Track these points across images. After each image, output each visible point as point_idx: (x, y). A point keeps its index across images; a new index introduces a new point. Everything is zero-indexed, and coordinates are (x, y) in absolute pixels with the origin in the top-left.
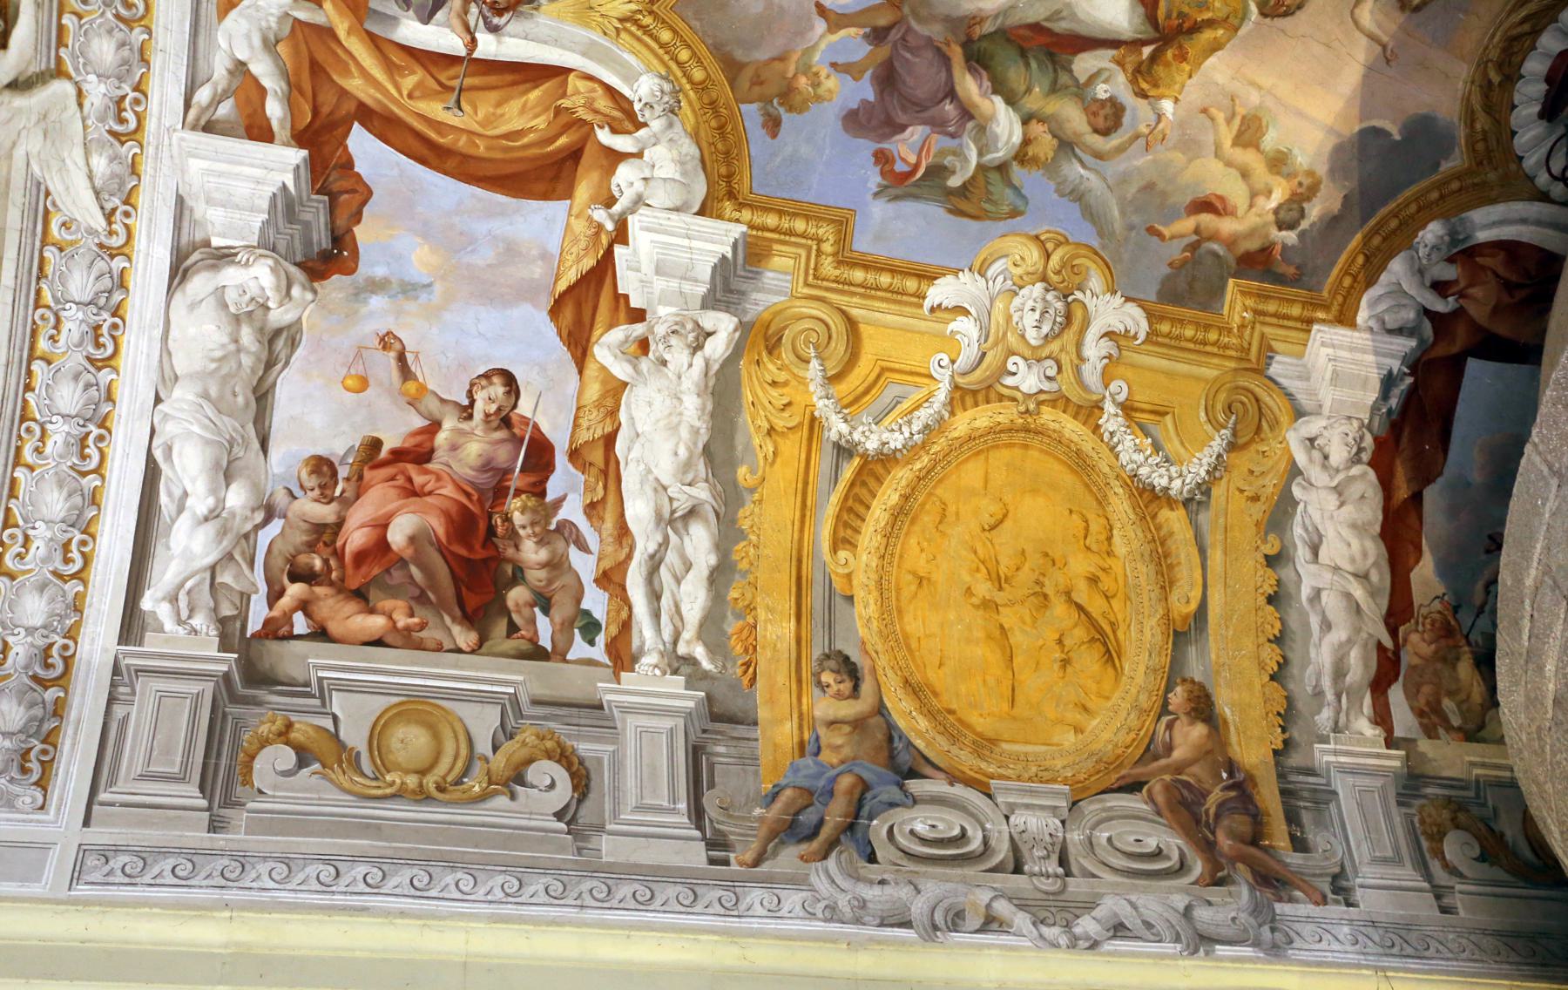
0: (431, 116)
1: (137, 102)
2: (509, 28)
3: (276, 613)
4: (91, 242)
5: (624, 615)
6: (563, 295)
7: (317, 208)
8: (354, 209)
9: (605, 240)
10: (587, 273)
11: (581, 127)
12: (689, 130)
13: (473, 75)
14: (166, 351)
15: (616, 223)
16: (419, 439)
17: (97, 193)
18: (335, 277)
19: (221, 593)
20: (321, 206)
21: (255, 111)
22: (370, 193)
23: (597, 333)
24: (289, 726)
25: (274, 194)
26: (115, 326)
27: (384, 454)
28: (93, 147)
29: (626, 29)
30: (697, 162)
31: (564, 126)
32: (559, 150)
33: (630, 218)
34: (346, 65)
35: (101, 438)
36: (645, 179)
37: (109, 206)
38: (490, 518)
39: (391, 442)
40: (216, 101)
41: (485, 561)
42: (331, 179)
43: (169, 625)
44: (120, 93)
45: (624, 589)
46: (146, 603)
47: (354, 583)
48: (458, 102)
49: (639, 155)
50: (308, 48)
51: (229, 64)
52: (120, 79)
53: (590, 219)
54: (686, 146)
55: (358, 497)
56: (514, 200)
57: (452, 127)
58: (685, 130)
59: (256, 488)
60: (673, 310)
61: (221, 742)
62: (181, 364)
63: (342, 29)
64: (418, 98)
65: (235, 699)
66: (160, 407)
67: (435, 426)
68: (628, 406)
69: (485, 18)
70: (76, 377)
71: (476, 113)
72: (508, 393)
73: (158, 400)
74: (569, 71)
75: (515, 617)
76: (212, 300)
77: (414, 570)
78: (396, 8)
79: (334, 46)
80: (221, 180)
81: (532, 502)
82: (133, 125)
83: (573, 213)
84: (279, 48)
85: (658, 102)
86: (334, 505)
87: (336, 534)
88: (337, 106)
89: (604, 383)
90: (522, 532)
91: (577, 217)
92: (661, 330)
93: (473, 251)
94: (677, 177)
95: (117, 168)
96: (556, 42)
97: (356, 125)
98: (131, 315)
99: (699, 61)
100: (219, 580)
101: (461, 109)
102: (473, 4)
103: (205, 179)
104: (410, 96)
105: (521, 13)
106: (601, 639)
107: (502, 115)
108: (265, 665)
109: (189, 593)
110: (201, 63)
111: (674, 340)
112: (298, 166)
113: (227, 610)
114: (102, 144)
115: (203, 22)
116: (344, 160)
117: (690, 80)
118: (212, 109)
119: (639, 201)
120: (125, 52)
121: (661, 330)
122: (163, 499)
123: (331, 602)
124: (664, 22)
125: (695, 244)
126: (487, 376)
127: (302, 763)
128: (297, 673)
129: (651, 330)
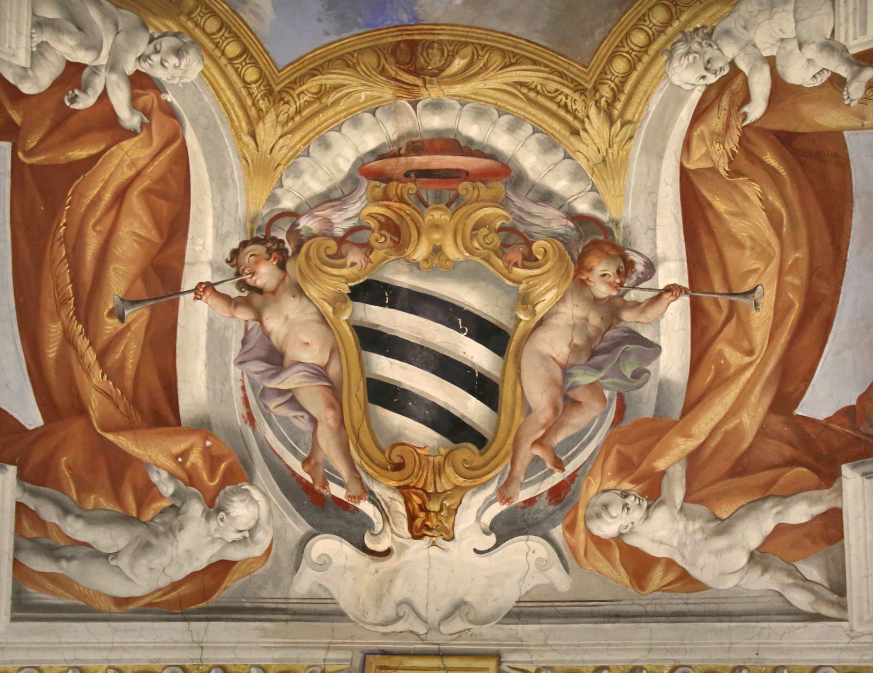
0: (770, 324)
2: (645, 251)
12: (728, 9)
13: (710, 283)
29: (621, 115)
31: (753, 163)
32: (783, 159)
33: (853, 51)
34: (727, 433)
36: (800, 46)
40: (804, 583)
48: (746, 294)
50: (716, 481)
51: (756, 573)
54: (750, 7)
57: (777, 297)
58: (730, 14)
63: (686, 445)
64: (750, 341)
69: (640, 281)
71: (755, 270)
74: (683, 171)
78: (648, 385)
79: (708, 451)
83: (859, 125)
84: (724, 516)
85: (702, 55)
88: (779, 438)
91: (863, 118)
94: (790, 7)
96: (653, 192)
97: (798, 412)
99: (642, 19)
101: (754, 290)
102: (626, 298)
104: (750, 353)
105: (625, 240)
107: (752, 238)
110: (761, 605)
112: (864, 474)
115: (713, 608)
117: (668, 23)
124: (604, 72)
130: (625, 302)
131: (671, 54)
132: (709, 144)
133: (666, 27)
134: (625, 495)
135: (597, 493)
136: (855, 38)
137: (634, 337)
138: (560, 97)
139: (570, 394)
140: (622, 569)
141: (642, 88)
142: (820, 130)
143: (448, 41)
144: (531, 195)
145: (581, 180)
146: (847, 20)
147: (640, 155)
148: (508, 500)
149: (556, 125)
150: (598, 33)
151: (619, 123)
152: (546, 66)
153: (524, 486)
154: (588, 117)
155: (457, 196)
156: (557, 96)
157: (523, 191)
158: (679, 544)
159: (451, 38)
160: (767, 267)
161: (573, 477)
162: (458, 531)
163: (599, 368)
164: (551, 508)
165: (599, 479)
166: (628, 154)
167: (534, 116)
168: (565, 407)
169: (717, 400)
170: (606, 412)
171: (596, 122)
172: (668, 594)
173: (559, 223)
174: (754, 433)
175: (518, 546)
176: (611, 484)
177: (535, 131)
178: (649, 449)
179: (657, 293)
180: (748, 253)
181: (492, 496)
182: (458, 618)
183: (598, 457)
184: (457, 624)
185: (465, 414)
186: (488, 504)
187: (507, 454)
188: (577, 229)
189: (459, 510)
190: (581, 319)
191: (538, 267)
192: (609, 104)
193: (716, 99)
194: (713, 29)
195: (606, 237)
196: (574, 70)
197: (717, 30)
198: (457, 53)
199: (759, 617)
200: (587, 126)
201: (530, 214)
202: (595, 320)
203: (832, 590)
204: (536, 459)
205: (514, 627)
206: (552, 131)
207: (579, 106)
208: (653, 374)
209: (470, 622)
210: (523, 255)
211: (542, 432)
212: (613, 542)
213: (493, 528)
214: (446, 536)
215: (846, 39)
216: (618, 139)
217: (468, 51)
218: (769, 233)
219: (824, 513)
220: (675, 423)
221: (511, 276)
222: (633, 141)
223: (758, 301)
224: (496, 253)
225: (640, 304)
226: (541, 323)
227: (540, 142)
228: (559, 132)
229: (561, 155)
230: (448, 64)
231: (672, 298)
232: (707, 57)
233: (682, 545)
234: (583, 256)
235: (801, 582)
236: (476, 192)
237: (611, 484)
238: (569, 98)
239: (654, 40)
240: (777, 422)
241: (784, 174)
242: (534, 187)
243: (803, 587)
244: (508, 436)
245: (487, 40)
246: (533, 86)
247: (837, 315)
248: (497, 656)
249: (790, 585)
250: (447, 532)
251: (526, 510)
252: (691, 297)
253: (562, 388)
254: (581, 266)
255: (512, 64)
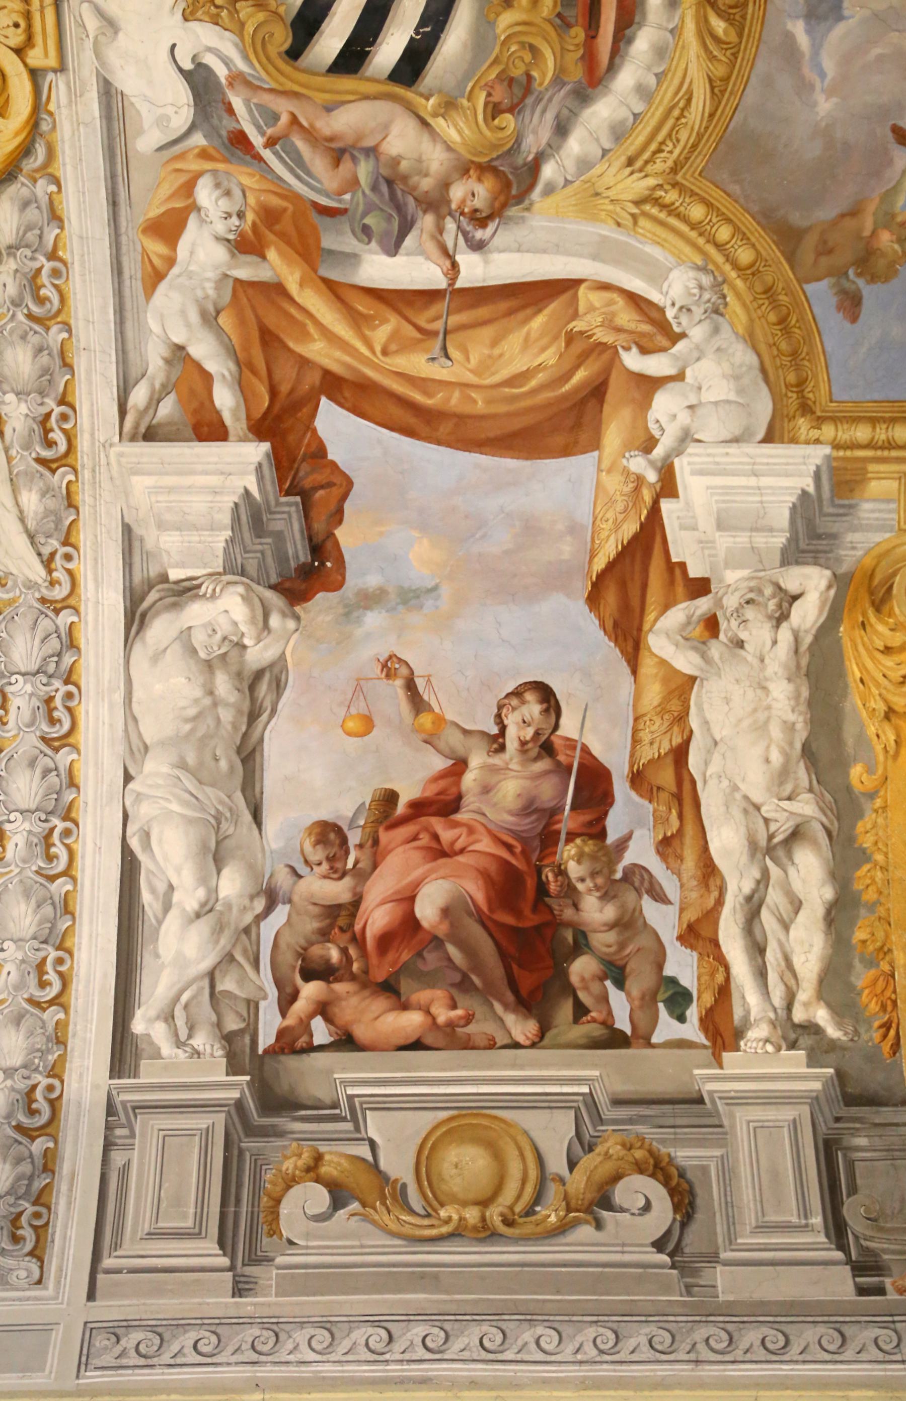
1: (64, 417)
2: (497, 241)
3: (290, 1021)
4: (32, 598)
5: (720, 978)
6: (601, 576)
7: (289, 513)
8: (333, 507)
9: (647, 496)
10: (629, 542)
11: (603, 352)
13: (459, 310)
14: (131, 718)
15: (659, 470)
16: (442, 784)
17: (31, 537)
18: (320, 596)
19: (224, 1003)
20: (293, 509)
21: (202, 404)
22: (350, 484)
23: (650, 617)
24: (318, 1158)
25: (236, 504)
26: (69, 696)
27: (401, 809)
28: (21, 481)
29: (645, 214)
30: (756, 373)
31: (579, 357)
33: (677, 462)
34: (303, 326)
35: (67, 833)
36: (691, 407)
37: (46, 551)
38: (539, 871)
39: (408, 793)
40: (155, 401)
41: (537, 928)
42: (301, 474)
43: (167, 1049)
44: (44, 410)
45: (717, 945)
46: (138, 1026)
47: (380, 974)
48: (444, 349)
49: (680, 377)
50: (257, 317)
51: (165, 352)
52: (42, 393)
53: (626, 472)
55: (375, 866)
56: (528, 463)
57: (440, 382)
58: (736, 334)
59: (253, 871)
60: (745, 573)
61: (239, 1186)
62: (150, 731)
65: (252, 1131)
66: (131, 786)
67: (460, 766)
68: (700, 709)
69: (465, 234)
70: (32, 764)
71: (468, 360)
72: (546, 711)
73: (128, 778)
74: (578, 282)
75: (582, 995)
76: (177, 647)
77: (452, 950)
78: (354, 242)
80: (173, 497)
81: (589, 847)
82: (62, 447)
84: (221, 320)
85: (697, 303)
86: (347, 881)
87: (353, 916)
88: (298, 380)
89: (665, 681)
90: (580, 886)
91: (609, 471)
92: (731, 601)
93: (483, 537)
95: (51, 503)
96: (558, 249)
97: (324, 400)
98: (87, 678)
100: (220, 987)
101: (447, 356)
102: (449, 219)
103: (153, 499)
104: (385, 352)
106: (693, 1013)
108: (283, 1086)
109: (186, 1007)
110: (132, 356)
111: (750, 613)
112: (260, 465)
113: (232, 1024)
114: (30, 476)
115: (128, 305)
116: (313, 448)
117: (736, 266)
118: (151, 412)
119: (686, 438)
120: (44, 359)
121: (731, 601)
122: (146, 896)
123: (354, 1001)
124: (693, 194)
125: (765, 481)
126: (517, 693)
127: (337, 1203)
128: (322, 1093)
129: (719, 603)
130: (444, 218)
131: (703, 269)
132: (603, 310)
133: (732, 264)
134: (241, 215)
135: (241, 184)
136: (689, 463)
137: (406, 227)
138: (671, 145)
139: (347, 157)
140: (162, 209)
141: (671, 237)
142: (604, 426)
143: (746, 13)
144: (565, 112)
145: (578, 168)
146: (709, 455)
147: (600, 235)
148: (231, 84)
149: (641, 139)
150: (736, 189)
151: (635, 210)
152: (707, 128)
153: (247, 102)
154: (646, 176)
155: (569, 26)
156: (671, 140)
157: (569, 103)
158: (191, 272)
159: (749, 17)
160: (471, 371)
161: (259, 158)
162: (193, 25)
163: (375, 188)
164: (224, 133)
165: (256, 186)
166: (602, 221)
167: (653, 114)
168: (333, 149)
169: (337, 316)
170: (327, 195)
171: (639, 185)
172: (140, 258)
173: (531, 145)
174: (303, 353)
175: (182, 94)
176: (251, 200)
177: (636, 116)
178: (289, 243)
179: (451, 253)
180: (486, 352)
181: (235, 66)
182: (99, 24)
183: (279, 186)
184: (92, 23)
185: (324, 35)
186: (226, 61)
187: (281, 84)
188: (525, 164)
189: (217, 28)
190: (428, 169)
191: (485, 120)
192: (656, 200)
193: (649, 318)
194: (722, 315)
195: (514, 197)
196: (698, 160)
197: (721, 319)
198: (731, 24)
199: (120, 353)
200: (636, 175)
201: (544, 111)
202: (426, 184)
203: (149, 428)
204: (276, 117)
205: (95, 87)
206: (634, 135)
207: (659, 166)
208: (367, 247)
209: (96, 38)
210: (500, 103)
211: (305, 124)
212: (190, 201)
213: (200, 66)
214: (188, 11)
215: (690, 455)
216: (618, 209)
217: (733, 37)
218: (505, 373)
219: (223, 423)
220: (315, 271)
221: (477, 90)
222: (615, 227)
223: (436, 362)
224: (503, 71)
225: (441, 234)
226: (424, 123)
227: (623, 122)
228: (632, 144)
229: (607, 146)
230: (720, 14)
231: (445, 269)
232: (693, 308)
233: (190, 275)
234: (494, 171)
235: (156, 396)
236: (572, 48)
237: (251, 200)
238: (668, 155)
239: (720, 251)
240: (313, 378)
241: (563, 390)
242: (574, 114)
243: (151, 399)
244: (302, 85)
245: (743, 59)
246: (686, 113)
247: (417, 442)
248: (62, 68)
249: (153, 385)
250: (192, 13)
251: (221, 105)
252: (446, 290)
253: (353, 147)
254: (485, 169)
255: (712, 88)
